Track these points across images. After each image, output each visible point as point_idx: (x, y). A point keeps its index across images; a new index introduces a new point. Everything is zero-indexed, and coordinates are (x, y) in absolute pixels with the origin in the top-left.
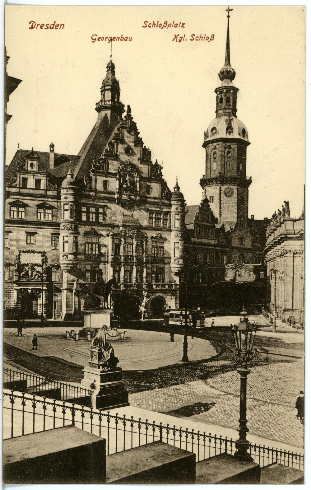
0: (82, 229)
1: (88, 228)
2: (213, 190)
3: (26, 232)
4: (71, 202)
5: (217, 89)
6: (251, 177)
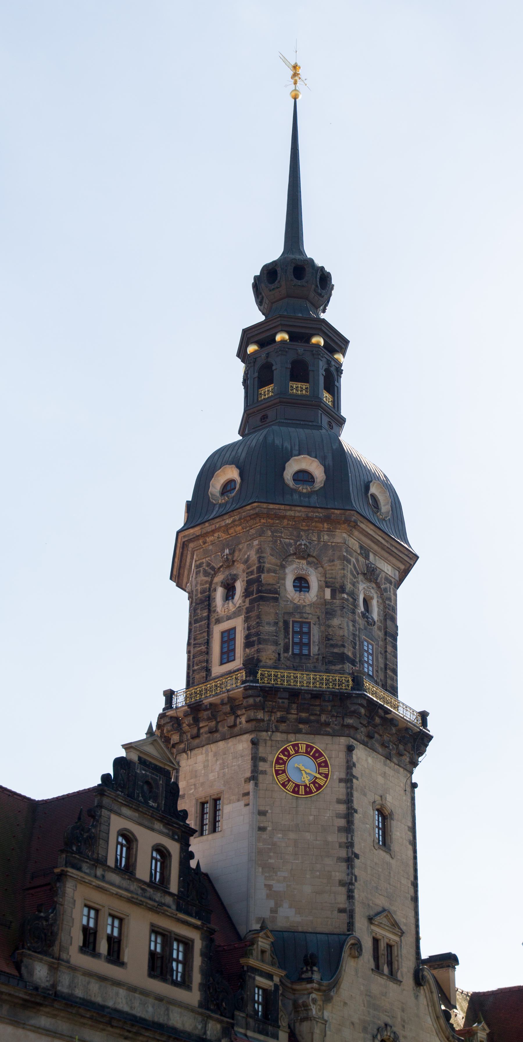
5: (245, 331)
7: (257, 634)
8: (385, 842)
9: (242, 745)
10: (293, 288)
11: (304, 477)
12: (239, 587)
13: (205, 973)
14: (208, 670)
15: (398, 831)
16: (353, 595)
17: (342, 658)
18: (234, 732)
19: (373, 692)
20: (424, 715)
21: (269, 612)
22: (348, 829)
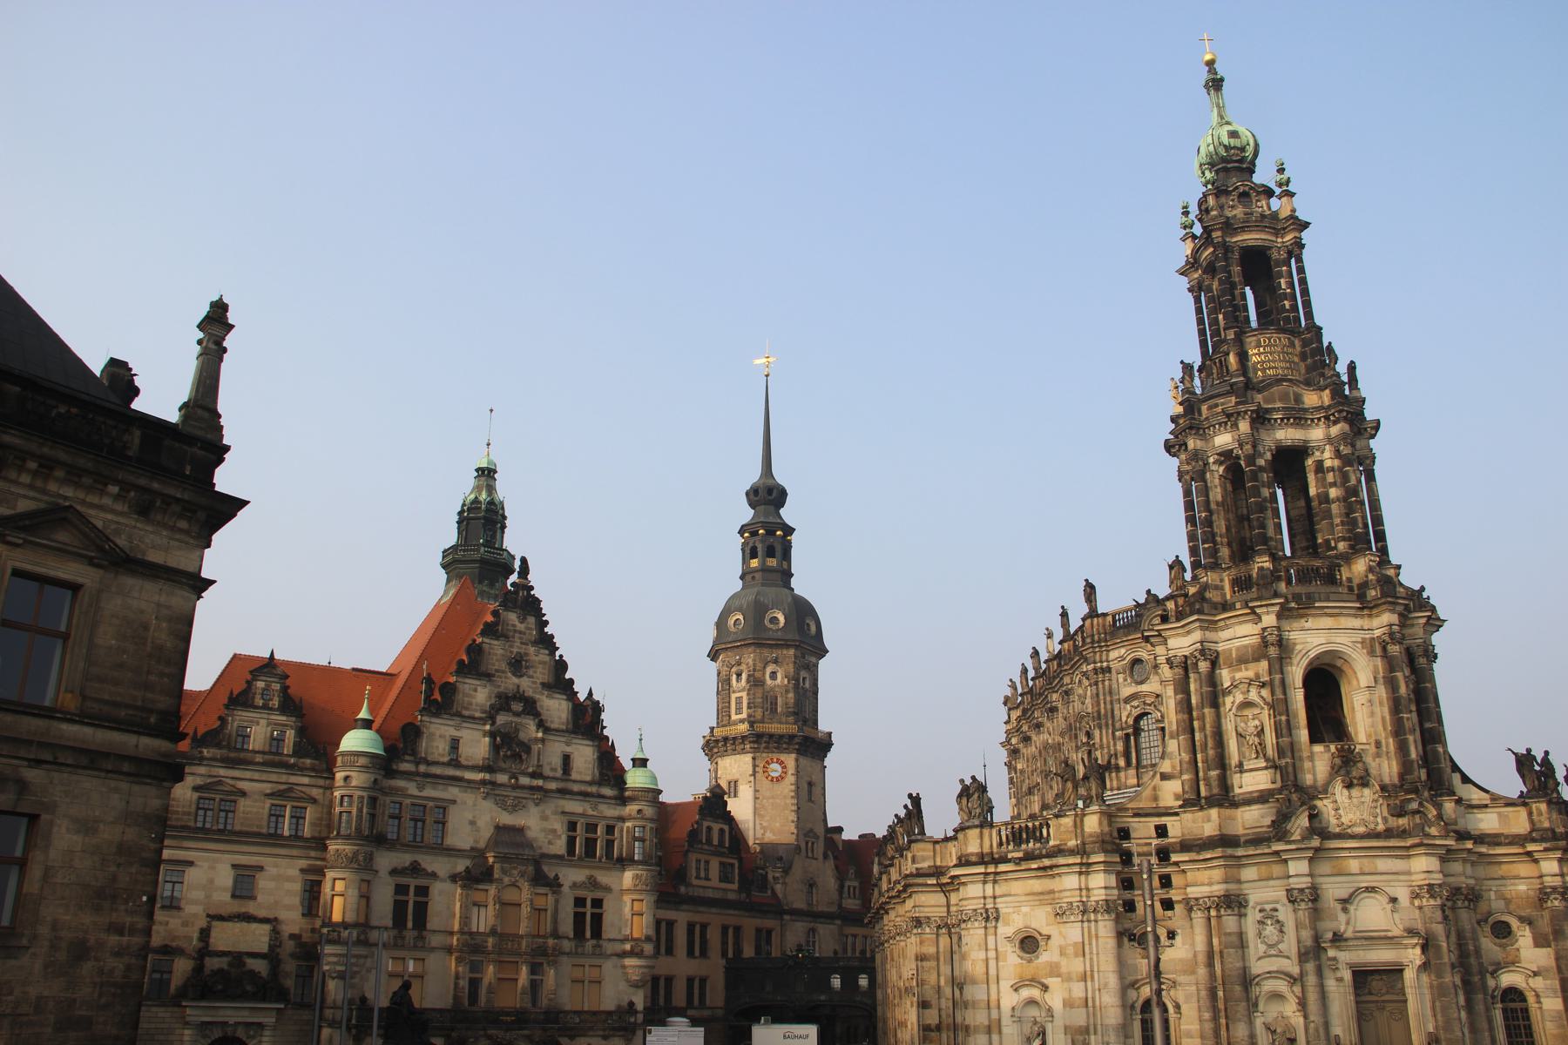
0: (386, 861)
1: (405, 859)
2: (736, 766)
3: (234, 866)
4: (363, 789)
6: (830, 734)
9: (748, 758)
10: (768, 496)
11: (774, 620)
12: (744, 676)
13: (740, 875)
16: (797, 680)
18: (743, 752)
19: (808, 731)
21: (759, 691)
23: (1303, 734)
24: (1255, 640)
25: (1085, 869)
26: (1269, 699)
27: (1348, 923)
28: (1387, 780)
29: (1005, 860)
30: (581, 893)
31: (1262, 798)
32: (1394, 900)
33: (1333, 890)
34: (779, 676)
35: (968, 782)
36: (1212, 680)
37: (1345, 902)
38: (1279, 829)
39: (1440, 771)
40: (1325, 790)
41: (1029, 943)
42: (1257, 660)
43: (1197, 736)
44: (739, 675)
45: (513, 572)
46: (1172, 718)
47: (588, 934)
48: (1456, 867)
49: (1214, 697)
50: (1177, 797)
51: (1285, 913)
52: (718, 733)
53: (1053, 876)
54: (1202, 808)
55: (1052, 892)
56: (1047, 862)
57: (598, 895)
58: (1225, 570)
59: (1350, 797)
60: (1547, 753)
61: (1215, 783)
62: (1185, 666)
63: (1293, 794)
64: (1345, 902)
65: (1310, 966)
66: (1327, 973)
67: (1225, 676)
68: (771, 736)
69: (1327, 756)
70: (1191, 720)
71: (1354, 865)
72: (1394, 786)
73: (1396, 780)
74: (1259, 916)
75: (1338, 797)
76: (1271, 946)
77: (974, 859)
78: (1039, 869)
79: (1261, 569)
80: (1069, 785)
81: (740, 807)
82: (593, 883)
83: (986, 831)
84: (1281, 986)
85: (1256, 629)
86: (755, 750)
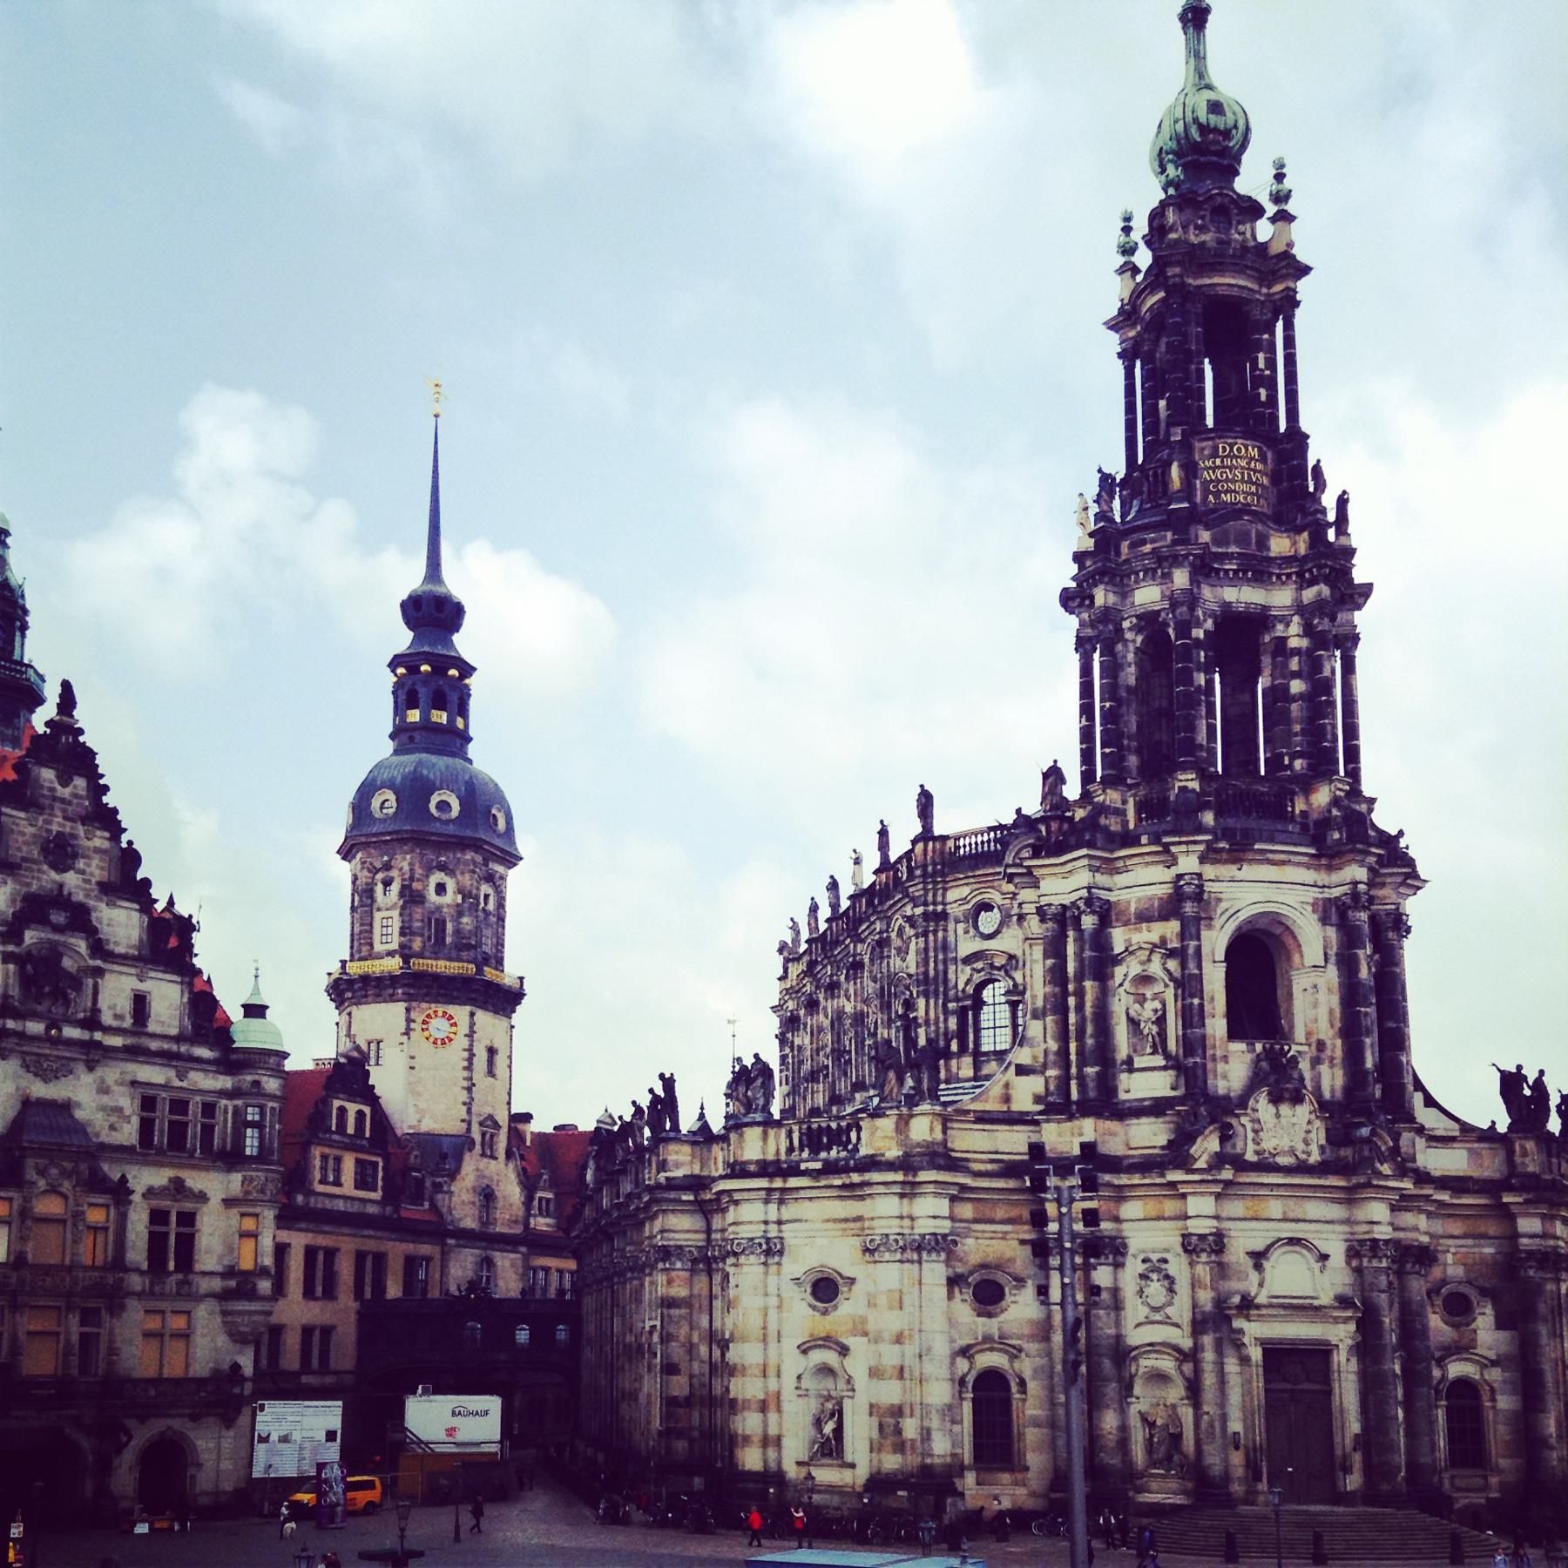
2: (380, 1020)
7: (410, 928)
8: (491, 1072)
14: (371, 945)
15: (501, 1060)
17: (469, 947)
18: (392, 999)
19: (489, 973)
20: (521, 979)
22: (469, 1068)
23: (1217, 1026)
24: (1165, 890)
25: (909, 1191)
26: (1177, 973)
27: (1261, 1285)
28: (1327, 1095)
29: (794, 1171)
30: (165, 1204)
31: (1157, 1108)
32: (1324, 1257)
33: (1243, 1239)
34: (451, 885)
35: (749, 1061)
36: (1100, 940)
37: (1258, 1258)
38: (1177, 1153)
39: (1402, 1087)
40: (1243, 1101)
41: (825, 1289)
42: (1164, 917)
43: (1072, 1018)
44: (387, 883)
45: (40, 701)
46: (1038, 989)
47: (171, 1265)
48: (1408, 1218)
49: (1102, 962)
50: (1038, 1099)
51: (1178, 1266)
52: (355, 969)
53: (862, 1198)
54: (1071, 1118)
55: (859, 1219)
56: (856, 1178)
57: (188, 1206)
58: (1130, 787)
59: (1278, 1116)
60: (1542, 1073)
61: (1091, 1085)
62: (1063, 919)
63: (1198, 1107)
64: (1258, 1258)
65: (1207, 1340)
66: (1230, 1352)
67: (1119, 938)
68: (436, 977)
69: (1249, 1057)
70: (1065, 994)
71: (1275, 1208)
72: (1339, 1103)
73: (1339, 1094)
74: (1141, 1268)
75: (1261, 1115)
76: (1155, 1309)
77: (752, 1168)
78: (843, 1187)
79: (1183, 789)
80: (892, 1075)
81: (386, 1079)
82: (178, 1186)
83: (772, 1132)
84: (1167, 1364)
85: (1168, 874)
86: (409, 998)
